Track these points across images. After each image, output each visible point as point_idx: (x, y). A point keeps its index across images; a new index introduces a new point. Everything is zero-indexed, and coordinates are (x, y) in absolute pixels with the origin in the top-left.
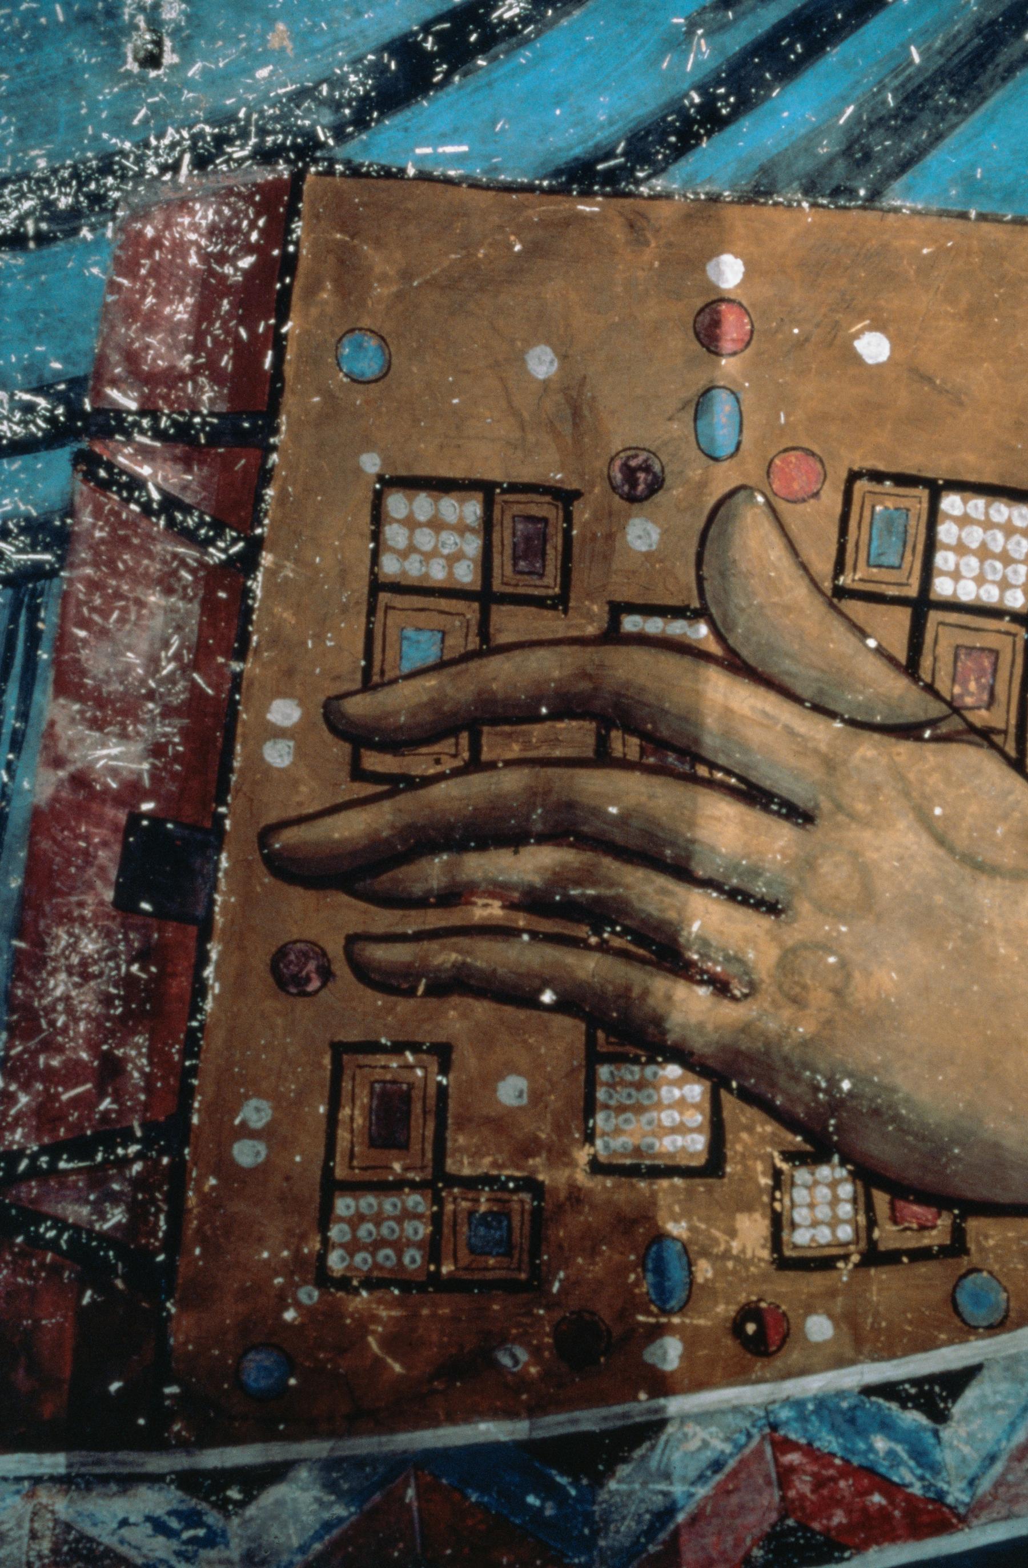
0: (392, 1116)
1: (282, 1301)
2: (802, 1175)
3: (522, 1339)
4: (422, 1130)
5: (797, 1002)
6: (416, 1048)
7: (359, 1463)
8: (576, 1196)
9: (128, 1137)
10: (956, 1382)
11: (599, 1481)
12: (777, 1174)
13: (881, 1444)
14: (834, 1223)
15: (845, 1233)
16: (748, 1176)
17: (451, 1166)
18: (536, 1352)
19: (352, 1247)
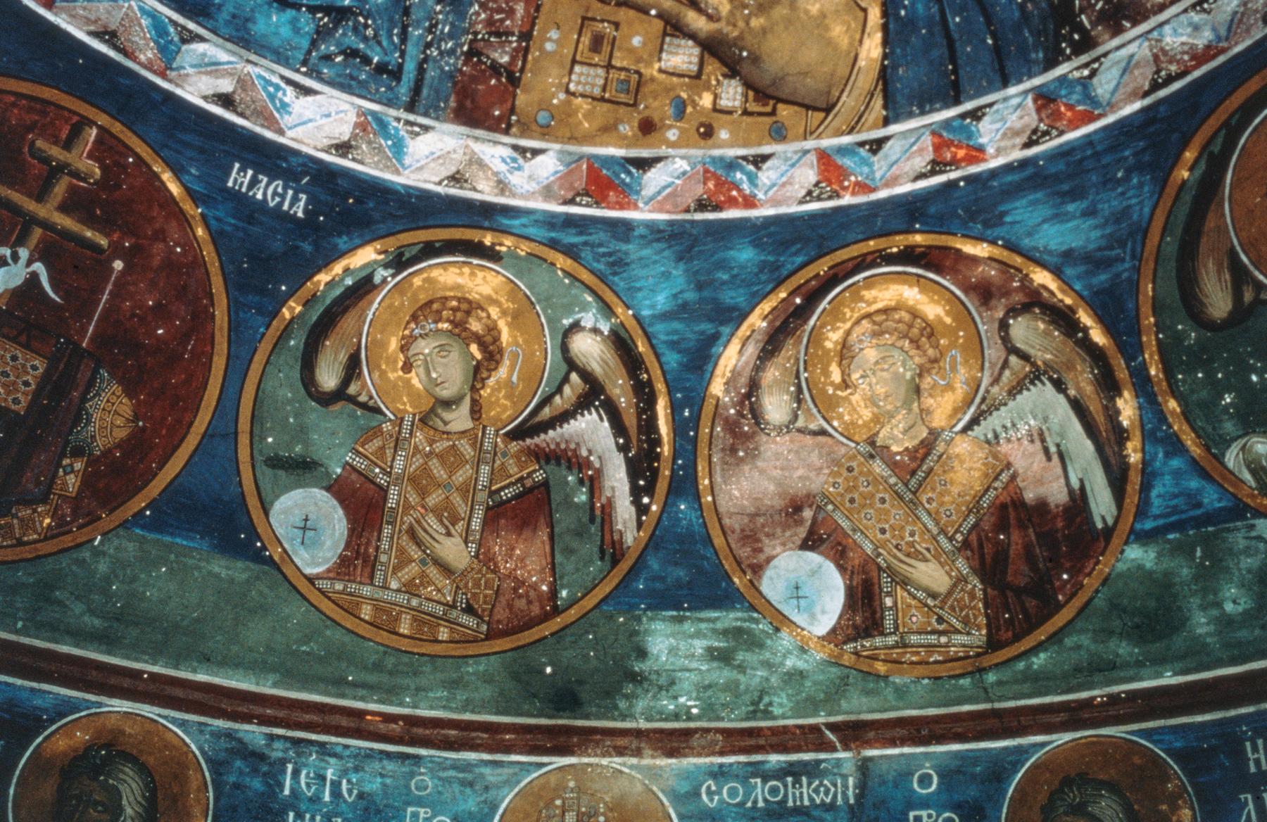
0: (597, 43)
1: (554, 96)
2: (726, 82)
3: (629, 122)
4: (606, 48)
5: (735, 25)
6: (609, 22)
7: (570, 154)
8: (652, 79)
9: (513, 34)
10: (765, 158)
11: (645, 171)
12: (718, 81)
13: (739, 175)
14: (735, 100)
15: (737, 103)
16: (709, 81)
17: (614, 62)
18: (632, 128)
19: (579, 83)
